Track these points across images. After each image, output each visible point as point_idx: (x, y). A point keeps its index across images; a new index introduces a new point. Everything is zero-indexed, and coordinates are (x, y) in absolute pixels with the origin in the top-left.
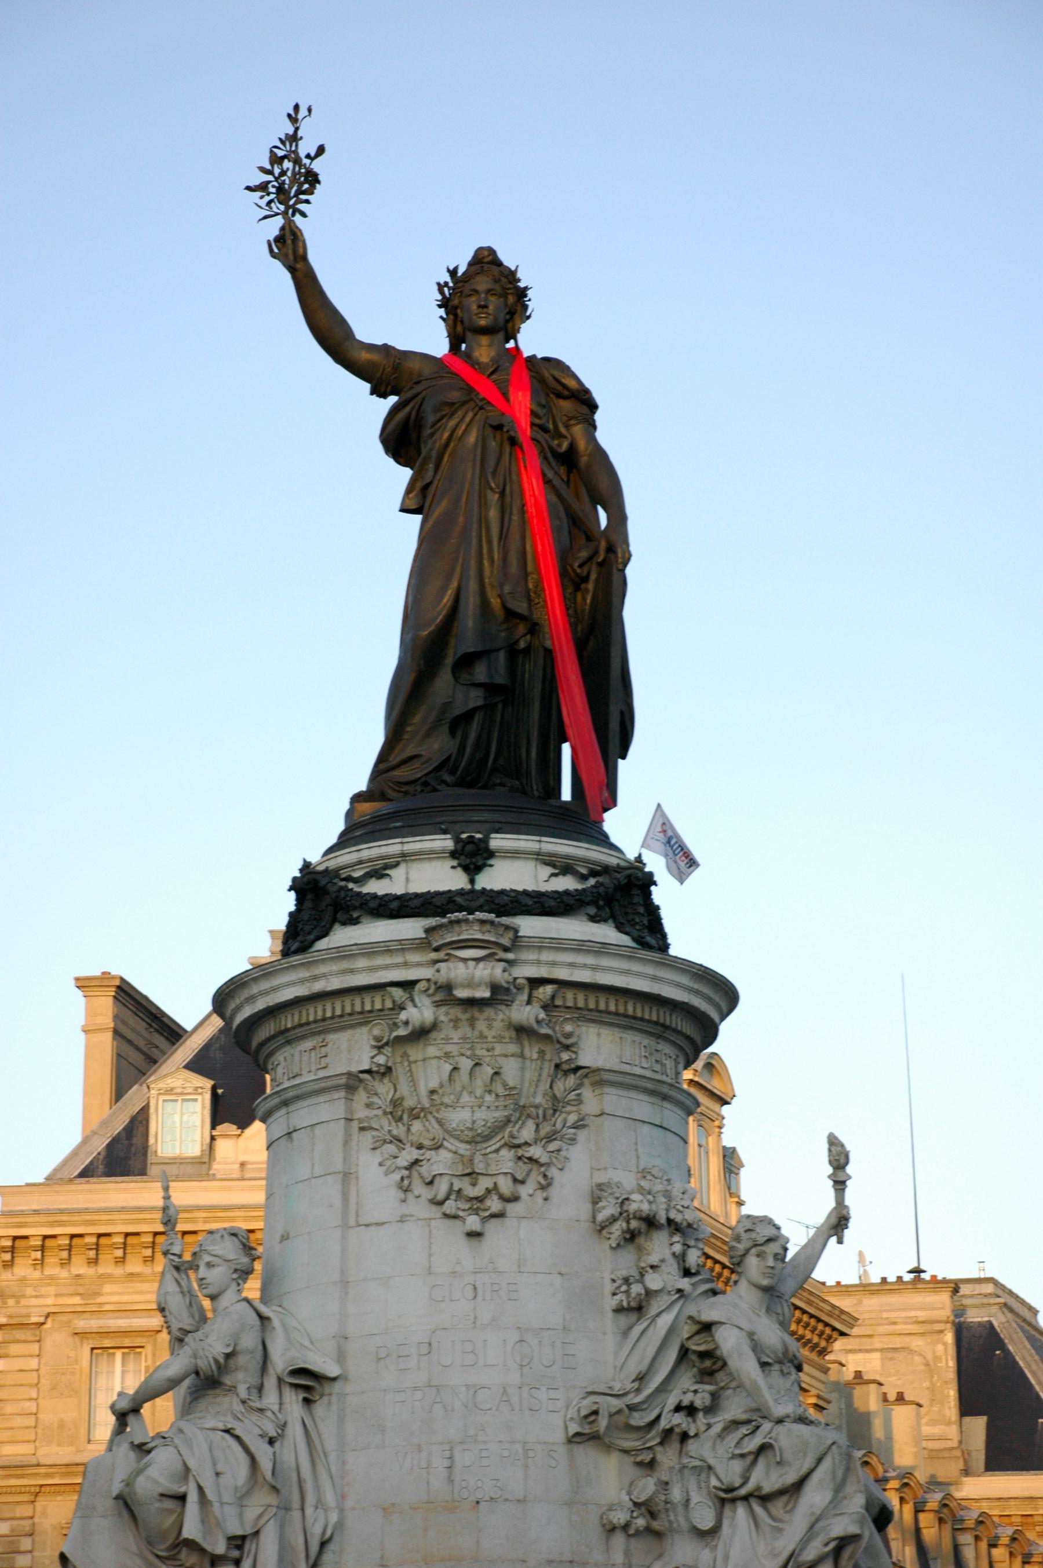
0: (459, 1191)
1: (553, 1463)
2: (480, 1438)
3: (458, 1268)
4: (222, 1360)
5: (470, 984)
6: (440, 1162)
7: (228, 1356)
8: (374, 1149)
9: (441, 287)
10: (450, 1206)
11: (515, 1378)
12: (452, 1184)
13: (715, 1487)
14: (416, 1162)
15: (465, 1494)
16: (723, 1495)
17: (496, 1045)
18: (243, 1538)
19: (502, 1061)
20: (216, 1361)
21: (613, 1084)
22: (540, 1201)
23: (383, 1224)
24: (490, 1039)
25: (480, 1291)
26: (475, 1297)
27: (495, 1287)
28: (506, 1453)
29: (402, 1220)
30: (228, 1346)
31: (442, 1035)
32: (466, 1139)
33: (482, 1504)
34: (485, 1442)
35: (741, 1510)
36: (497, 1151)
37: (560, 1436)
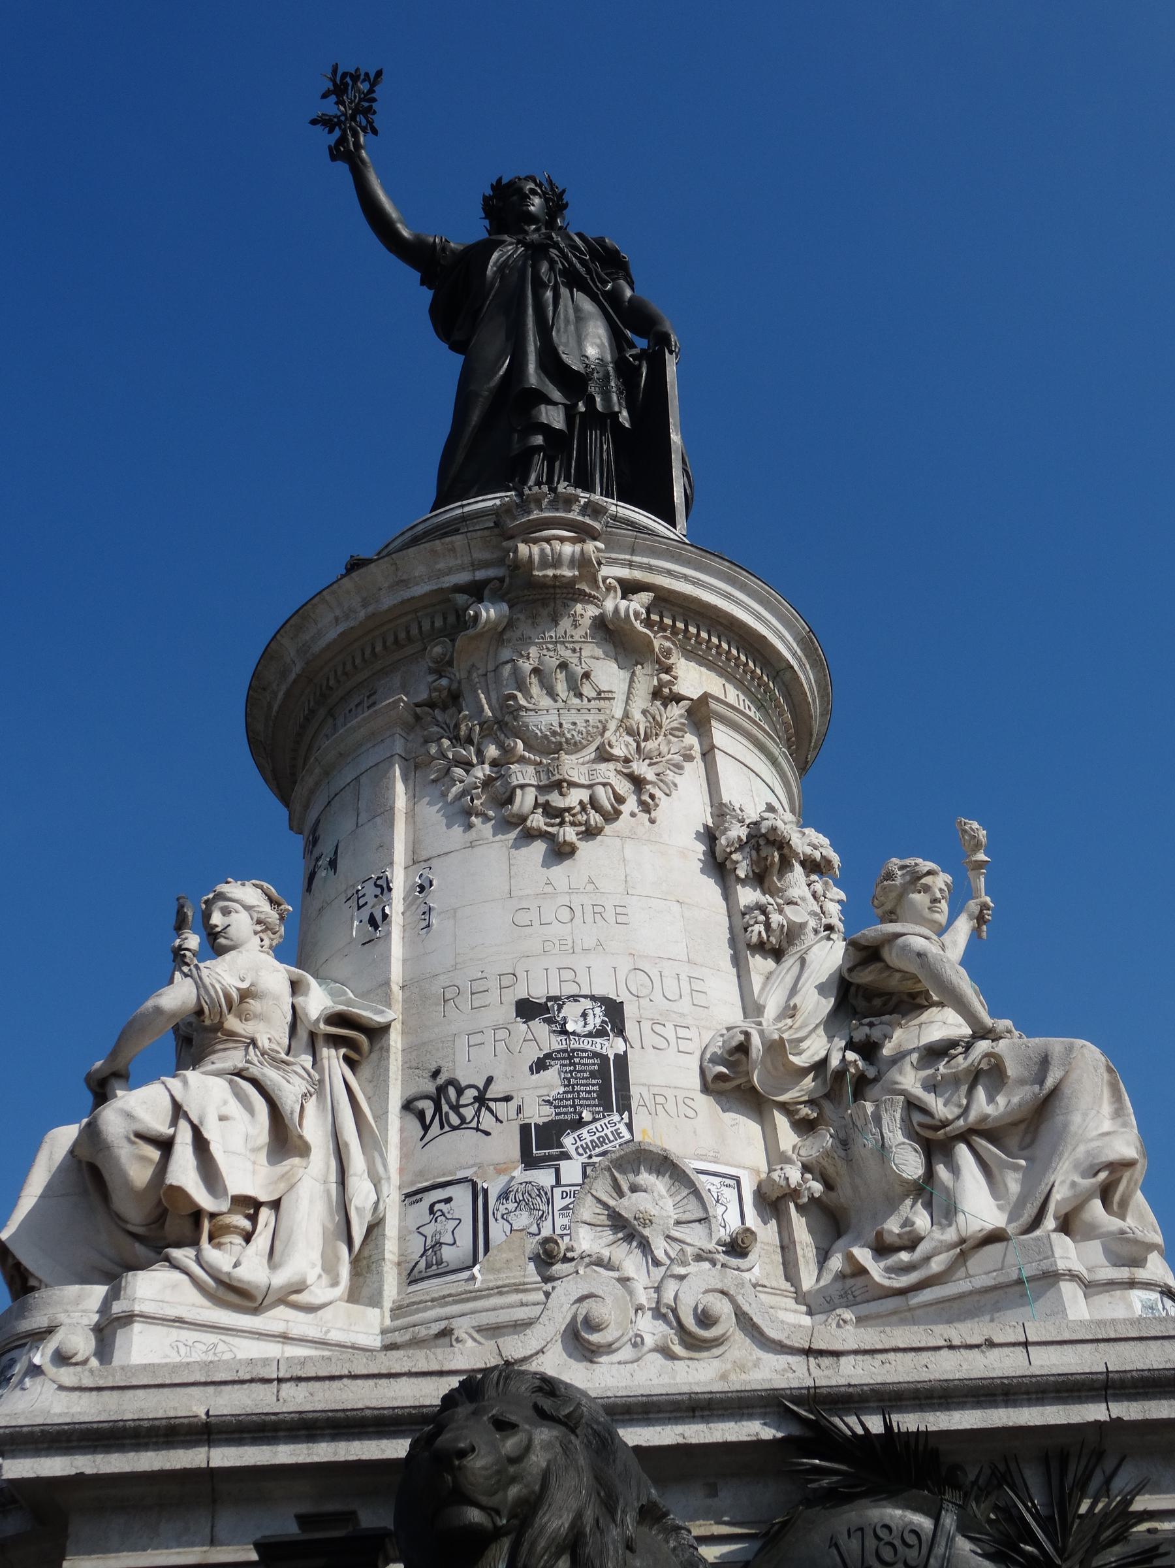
1: (691, 1114)
4: (235, 995)
5: (557, 562)
7: (246, 995)
9: (486, 199)
10: (537, 820)
13: (921, 1125)
16: (929, 1134)
17: (584, 646)
18: (257, 1205)
19: (590, 661)
20: (228, 997)
21: (723, 720)
24: (576, 638)
25: (578, 913)
27: (597, 909)
29: (472, 845)
31: (518, 634)
35: (963, 1152)
37: (696, 1082)
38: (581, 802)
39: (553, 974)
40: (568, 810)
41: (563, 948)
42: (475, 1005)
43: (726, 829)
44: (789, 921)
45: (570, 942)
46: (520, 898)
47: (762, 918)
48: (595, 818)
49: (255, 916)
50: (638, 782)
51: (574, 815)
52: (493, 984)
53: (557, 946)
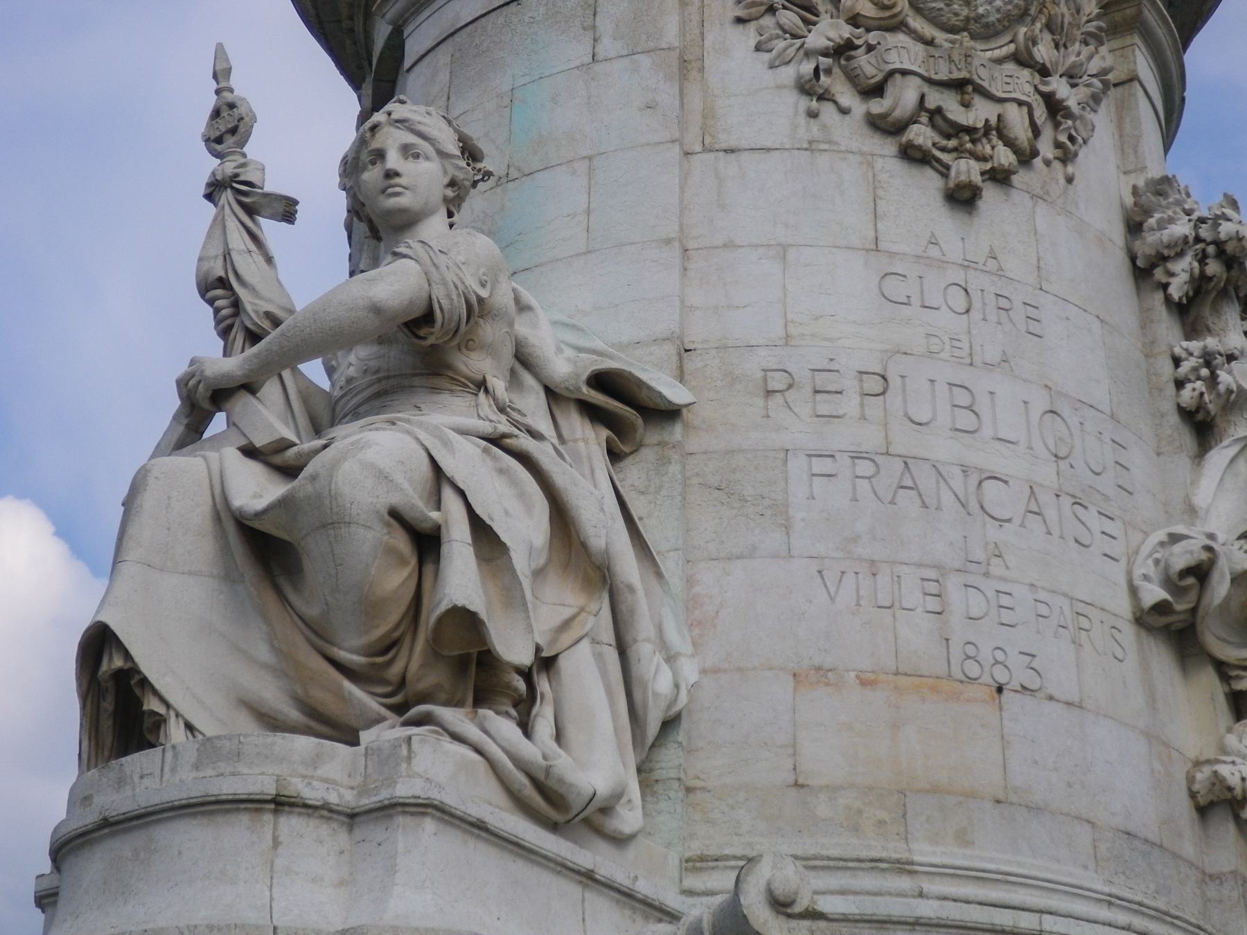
0: (939, 111)
2: (992, 570)
3: (934, 252)
6: (901, 51)
8: (740, 21)
10: (922, 134)
11: (1046, 474)
12: (922, 97)
14: (842, 50)
15: (974, 670)
22: (1062, 181)
23: (769, 150)
25: (977, 305)
26: (968, 311)
27: (1003, 303)
28: (1043, 610)
29: (810, 147)
30: (483, 285)
32: (954, 21)
33: (1006, 694)
34: (1003, 579)
36: (999, 61)
38: (987, 121)
39: (942, 389)
40: (970, 130)
41: (957, 353)
42: (824, 409)
43: (1171, 220)
44: (1239, 386)
45: (966, 346)
46: (892, 255)
47: (1205, 372)
48: (1005, 157)
49: (452, 172)
50: (1054, 107)
51: (973, 141)
52: (850, 384)
53: (947, 347)
